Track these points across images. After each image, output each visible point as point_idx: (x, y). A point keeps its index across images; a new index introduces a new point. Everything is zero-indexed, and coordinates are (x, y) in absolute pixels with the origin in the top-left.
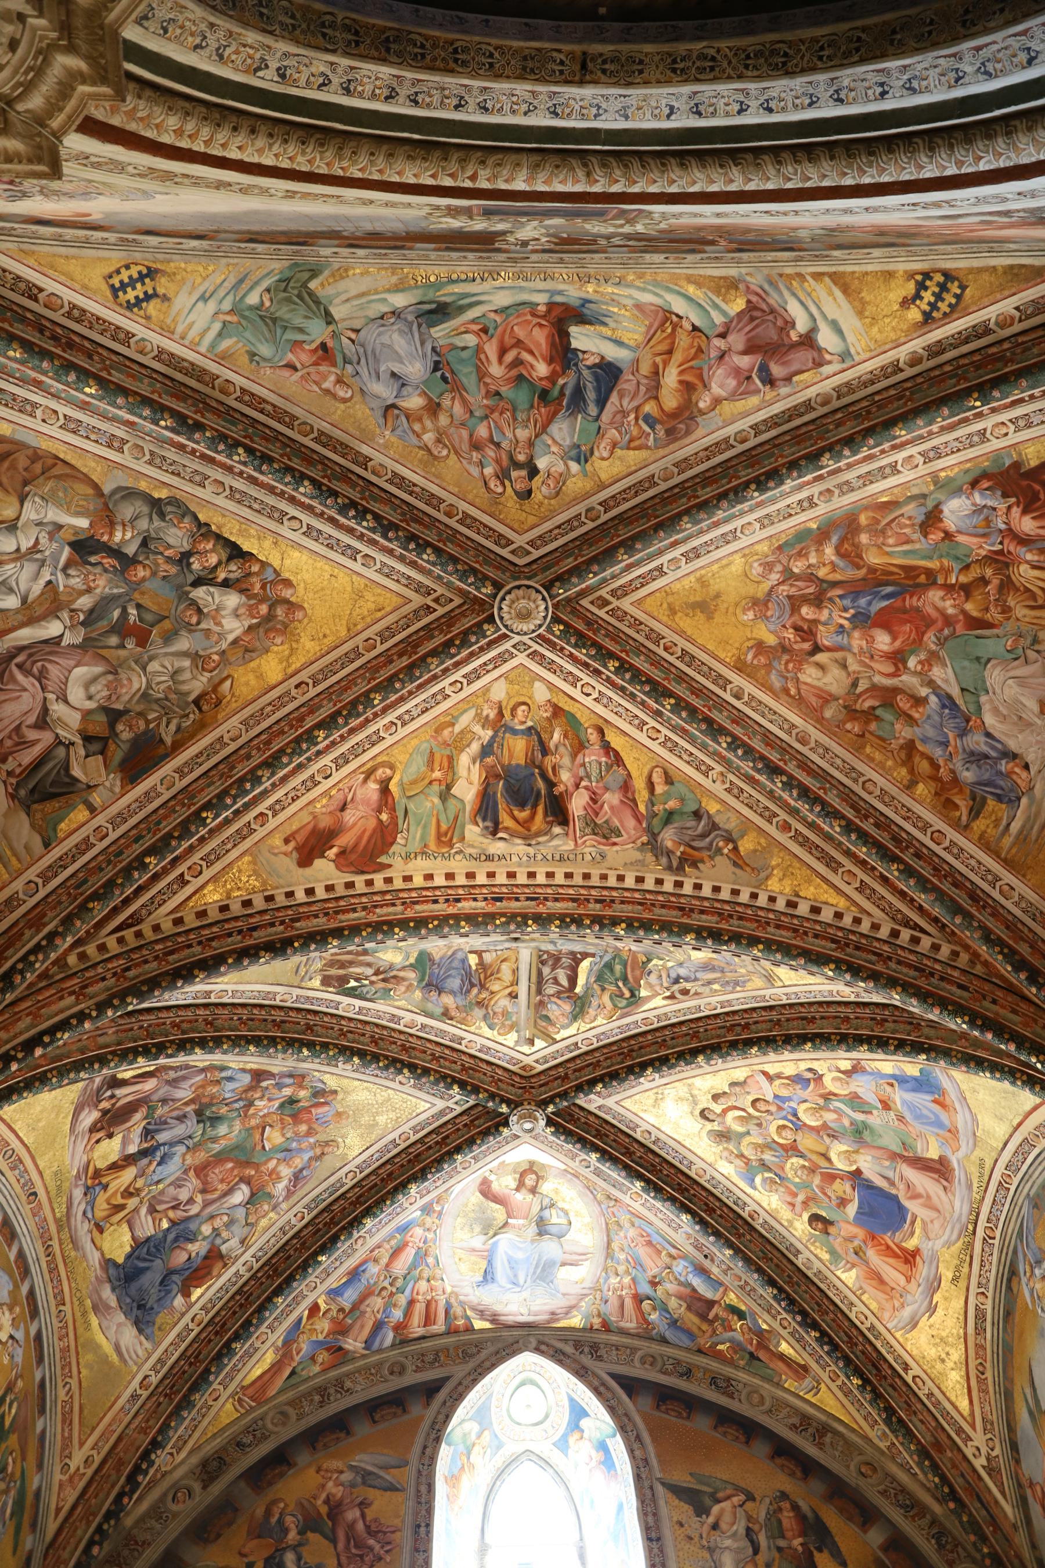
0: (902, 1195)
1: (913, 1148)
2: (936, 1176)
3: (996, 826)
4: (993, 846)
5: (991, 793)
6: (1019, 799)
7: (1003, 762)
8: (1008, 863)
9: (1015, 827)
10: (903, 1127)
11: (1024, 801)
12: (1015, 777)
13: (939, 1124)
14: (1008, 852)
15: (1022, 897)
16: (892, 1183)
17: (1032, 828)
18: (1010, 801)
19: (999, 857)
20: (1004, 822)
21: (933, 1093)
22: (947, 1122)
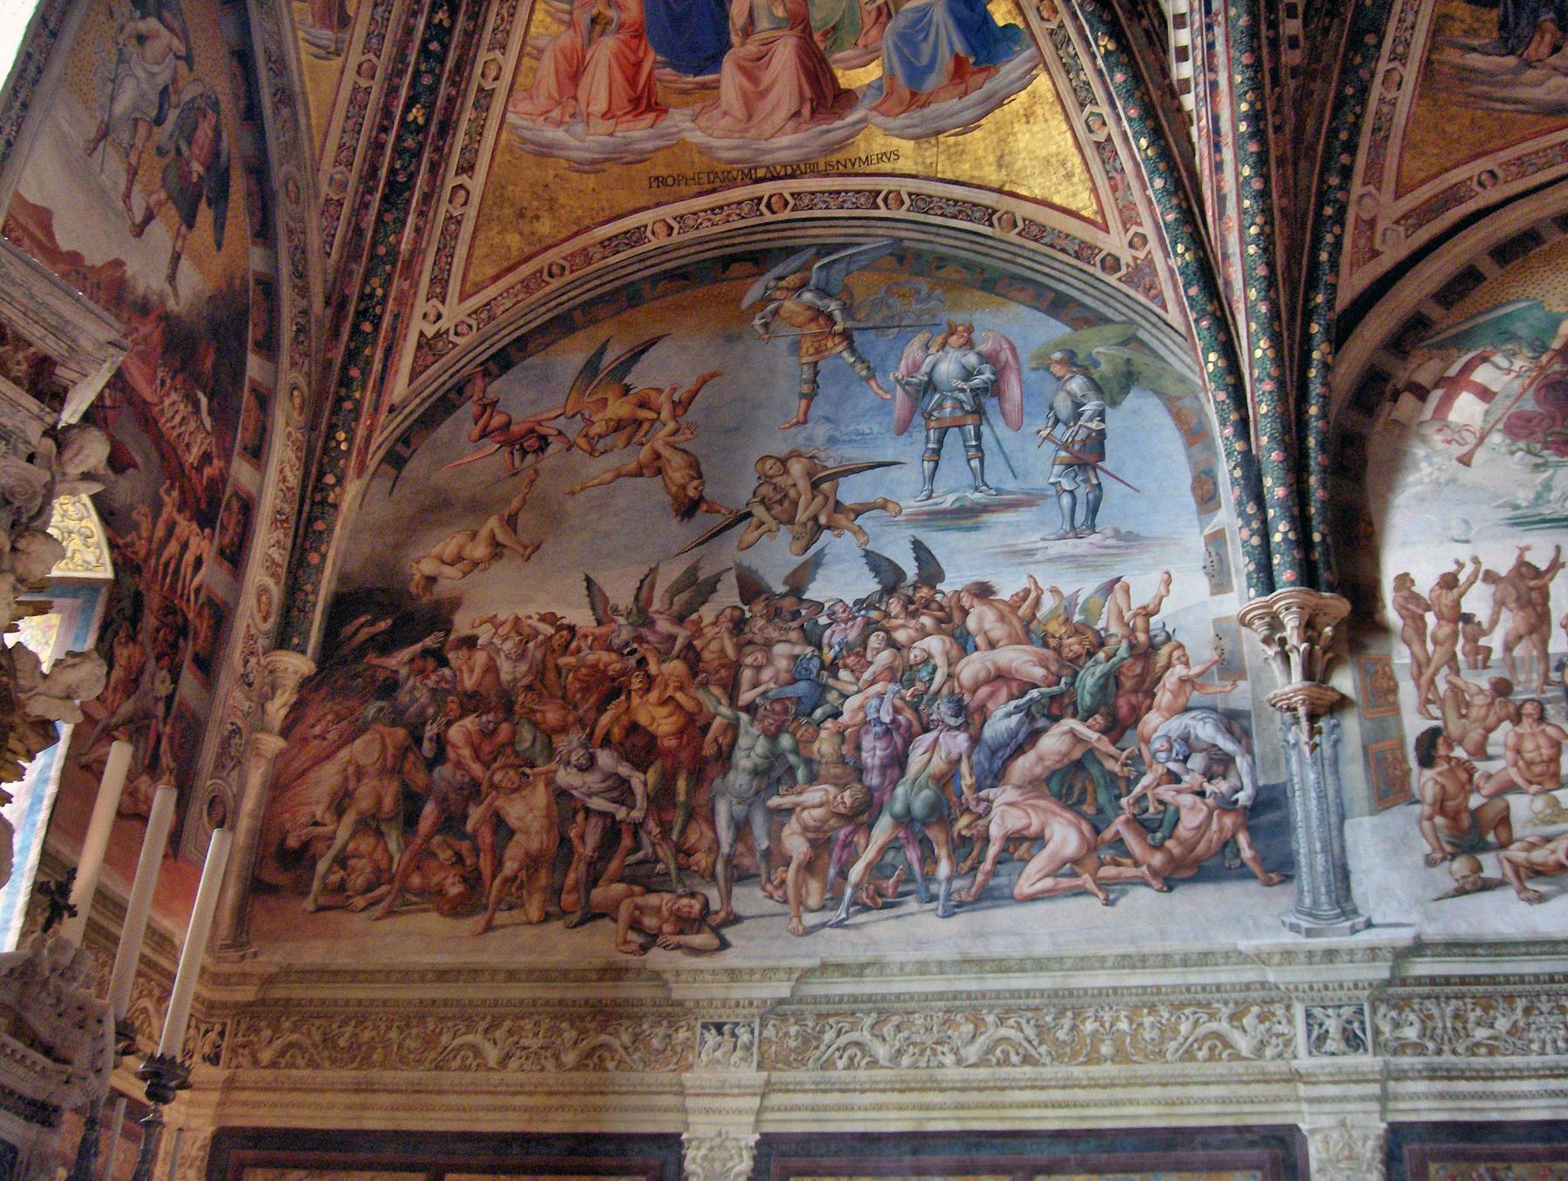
0: (740, 50)
1: (837, 45)
2: (808, 93)
3: (1466, 33)
4: (1439, 38)
5: (1506, 11)
6: (1512, 52)
7: (1551, 15)
8: (1428, 68)
9: (1475, 60)
10: (869, 20)
11: (1511, 61)
12: (1537, 38)
13: (916, 74)
14: (1442, 63)
15: (1393, 103)
16: (748, 30)
17: (1483, 83)
18: (1506, 41)
19: (1430, 52)
20: (1476, 43)
21: (973, 51)
22: (932, 82)
